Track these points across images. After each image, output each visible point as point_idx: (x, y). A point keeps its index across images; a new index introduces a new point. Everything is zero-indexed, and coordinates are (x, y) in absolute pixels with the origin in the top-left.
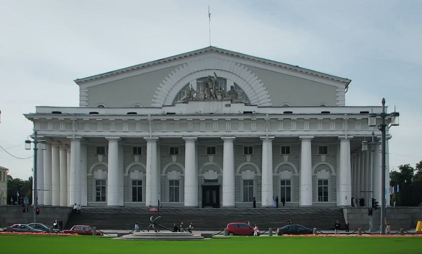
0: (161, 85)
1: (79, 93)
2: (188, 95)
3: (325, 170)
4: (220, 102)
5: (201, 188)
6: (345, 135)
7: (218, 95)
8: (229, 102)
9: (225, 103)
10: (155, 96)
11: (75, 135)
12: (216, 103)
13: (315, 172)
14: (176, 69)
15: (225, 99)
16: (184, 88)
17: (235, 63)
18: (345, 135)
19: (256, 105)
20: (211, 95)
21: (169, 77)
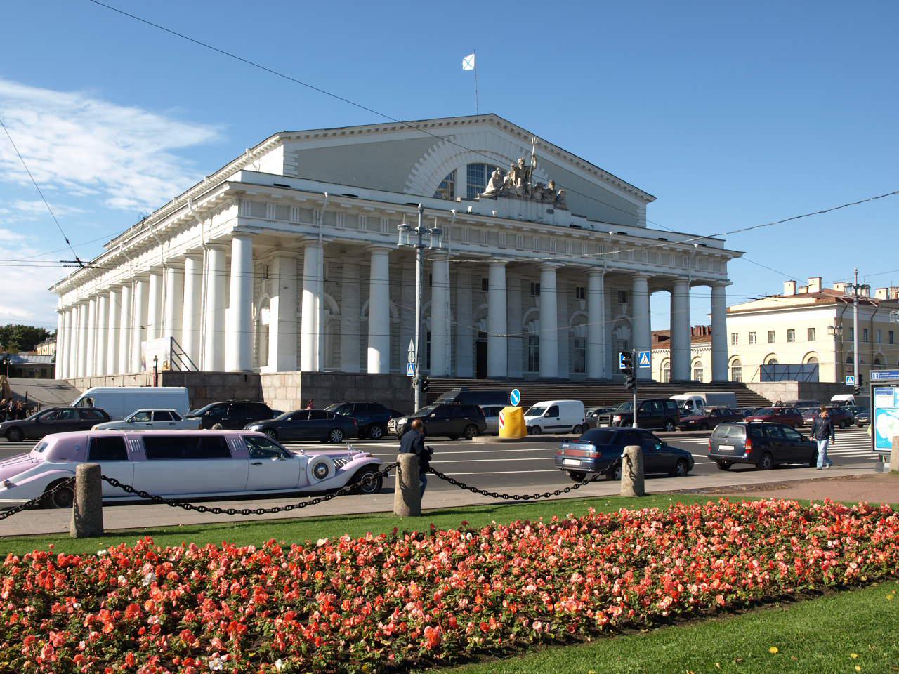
0: (417, 165)
1: (283, 158)
2: (495, 185)
3: (626, 327)
4: (539, 205)
5: (475, 347)
6: (688, 276)
7: (536, 192)
8: (551, 207)
9: (547, 207)
10: (407, 183)
11: (324, 236)
12: (534, 204)
13: (615, 329)
14: (440, 143)
15: (546, 200)
16: (447, 178)
17: (519, 149)
18: (688, 276)
19: (586, 217)
20: (527, 192)
21: (429, 154)
